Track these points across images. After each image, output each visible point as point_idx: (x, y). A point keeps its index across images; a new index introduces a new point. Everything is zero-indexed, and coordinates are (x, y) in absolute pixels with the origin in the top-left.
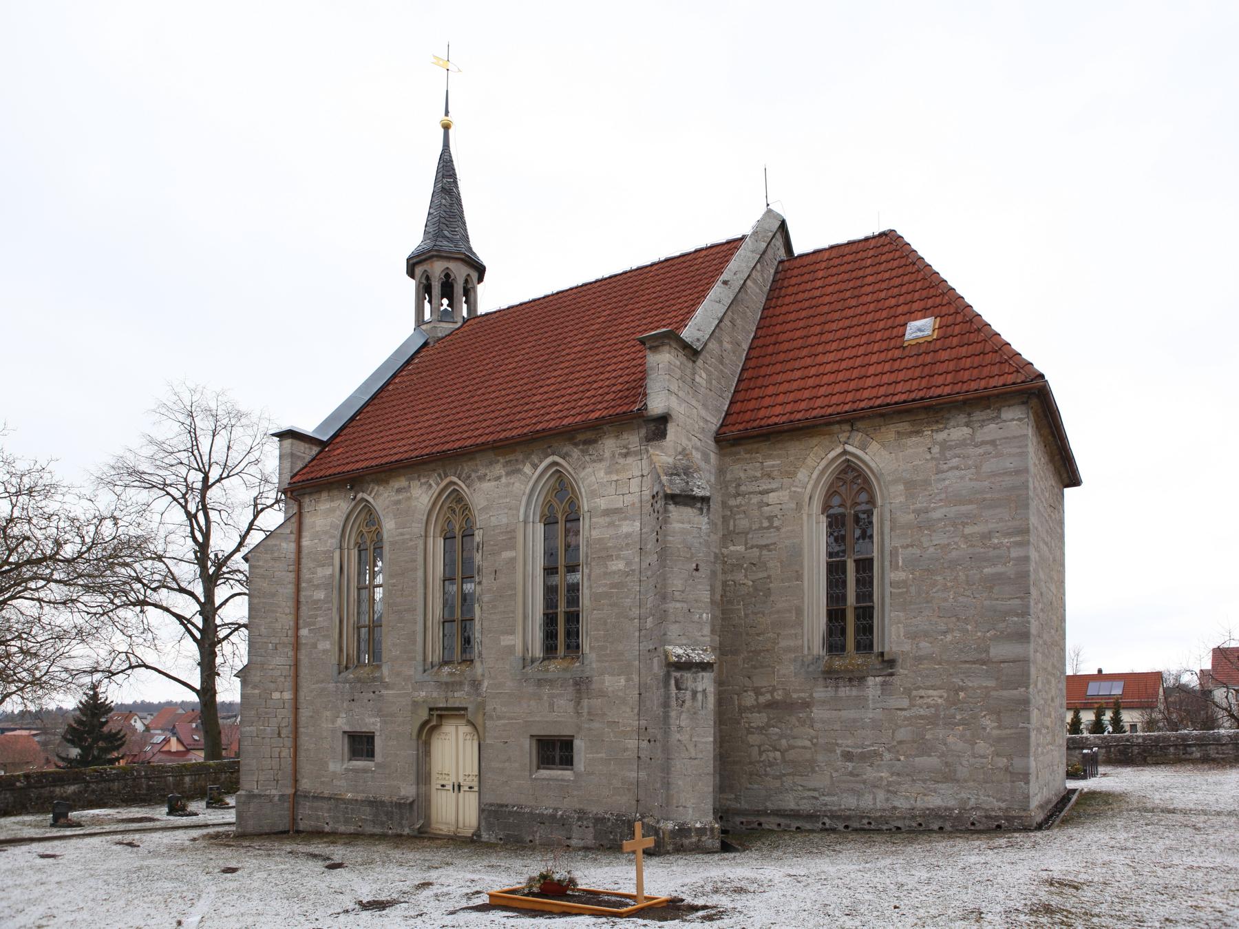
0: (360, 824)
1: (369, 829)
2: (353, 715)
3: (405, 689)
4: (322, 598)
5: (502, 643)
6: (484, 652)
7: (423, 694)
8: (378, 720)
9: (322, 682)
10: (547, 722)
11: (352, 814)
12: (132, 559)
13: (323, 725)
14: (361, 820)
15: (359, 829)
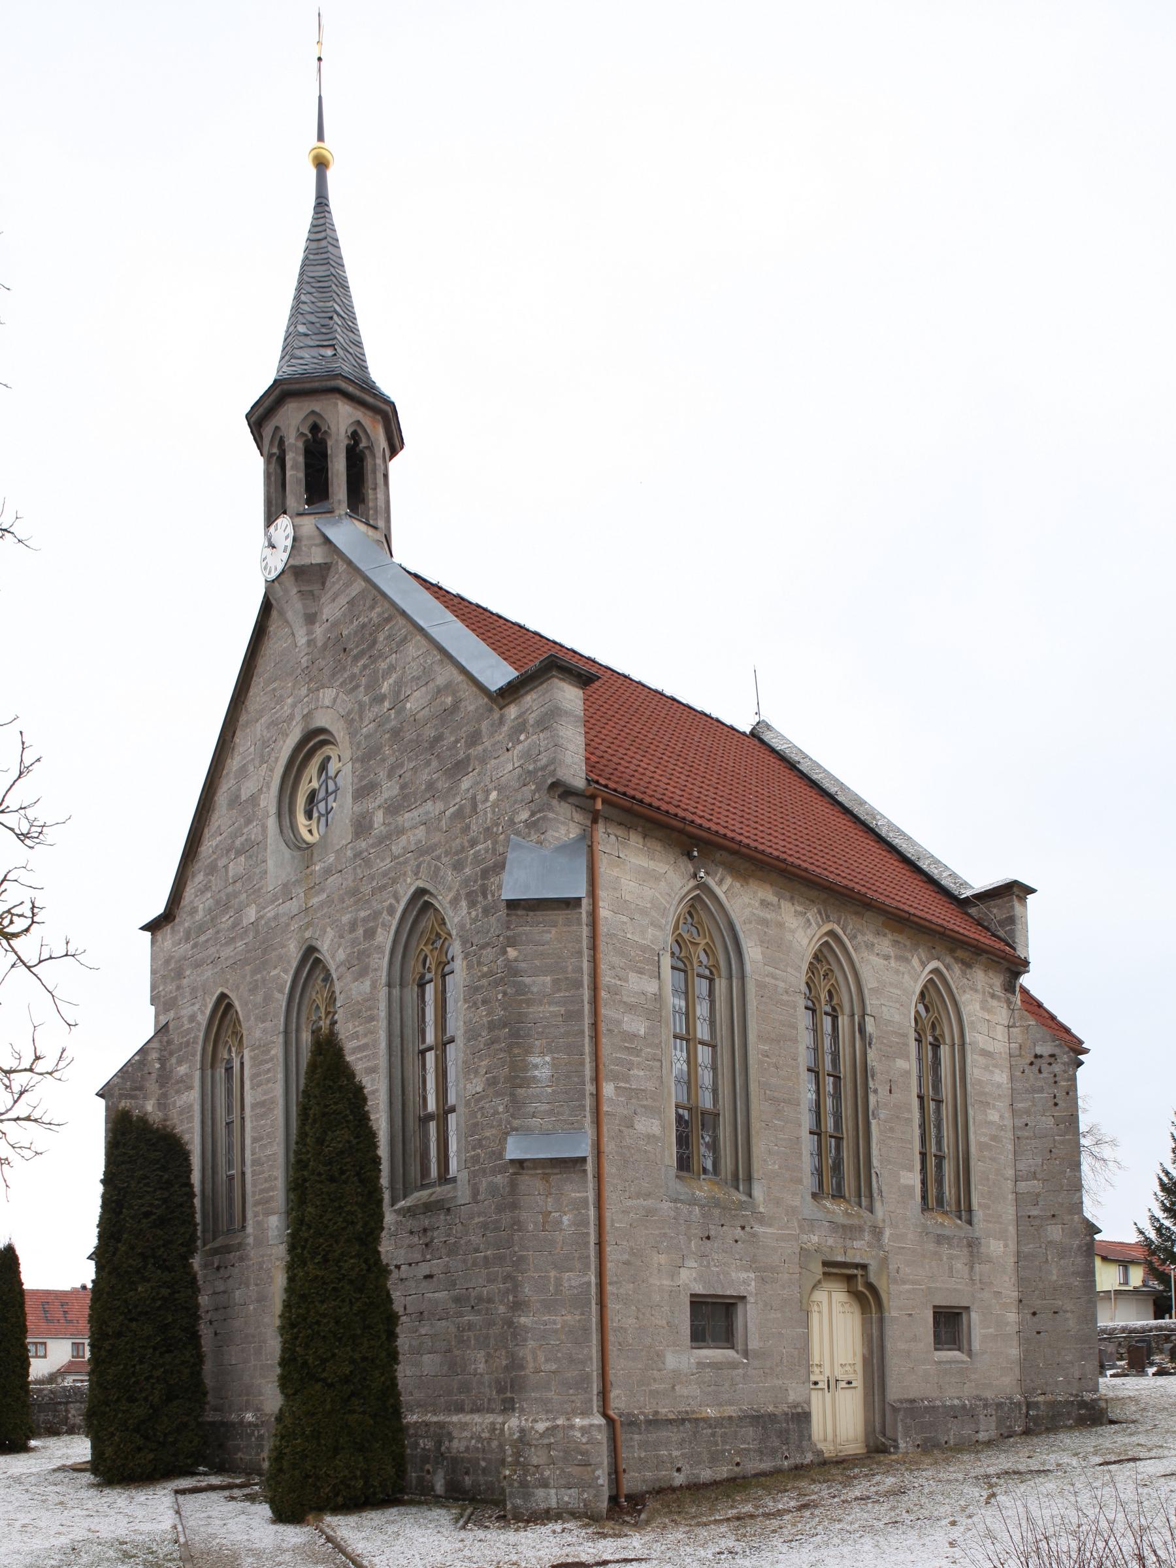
0: (738, 1459)
1: (754, 1465)
2: (708, 1266)
3: (788, 1228)
4: (642, 1032)
5: (902, 1181)
6: (884, 1188)
7: (815, 1239)
8: (752, 1275)
9: (648, 1195)
10: (947, 1289)
11: (724, 1442)
12: (269, 689)
13: (651, 1281)
14: (739, 1452)
15: (736, 1469)
